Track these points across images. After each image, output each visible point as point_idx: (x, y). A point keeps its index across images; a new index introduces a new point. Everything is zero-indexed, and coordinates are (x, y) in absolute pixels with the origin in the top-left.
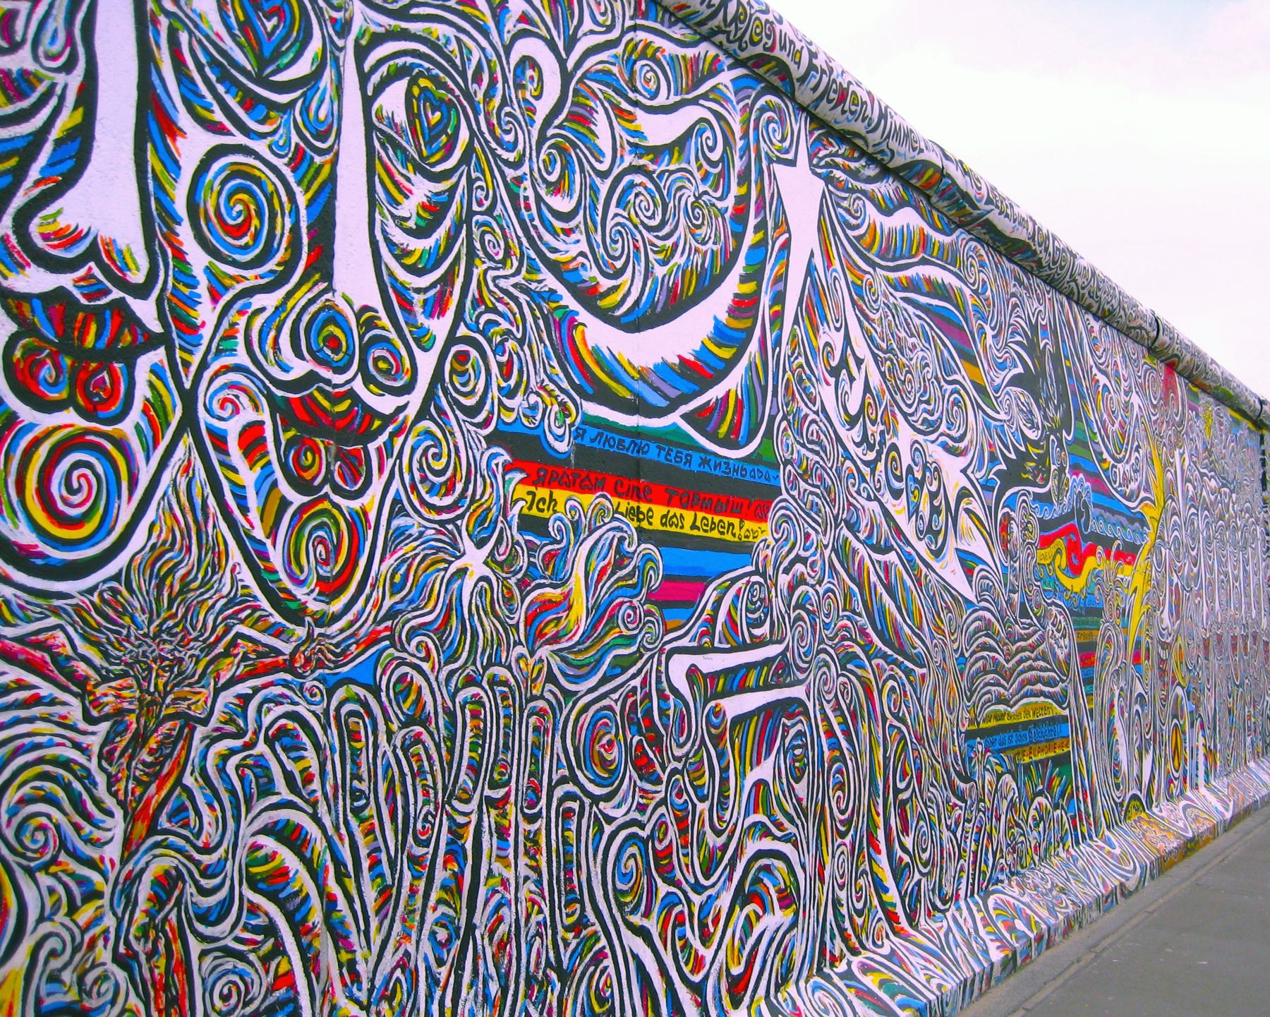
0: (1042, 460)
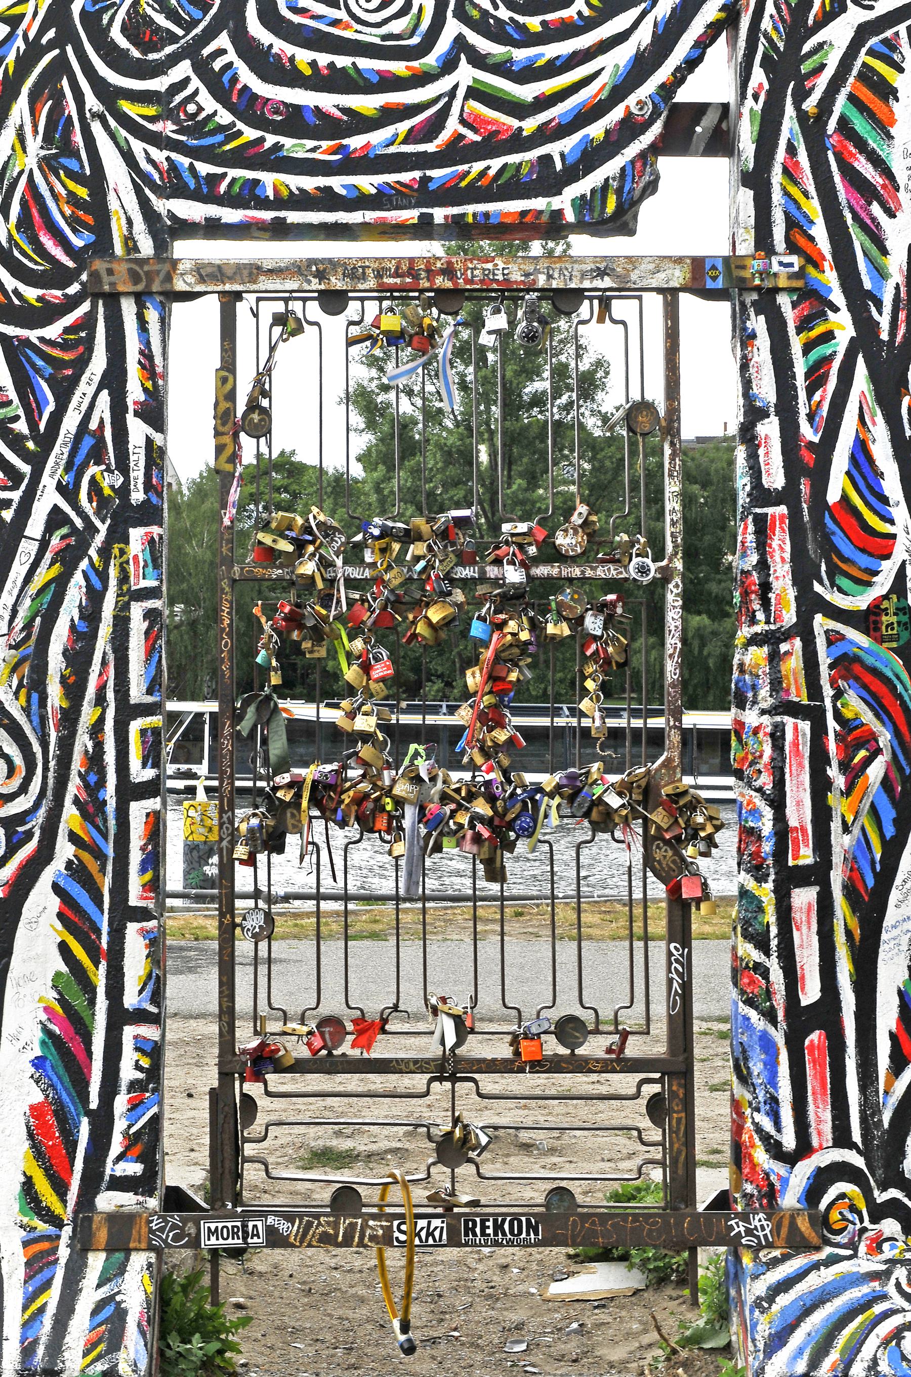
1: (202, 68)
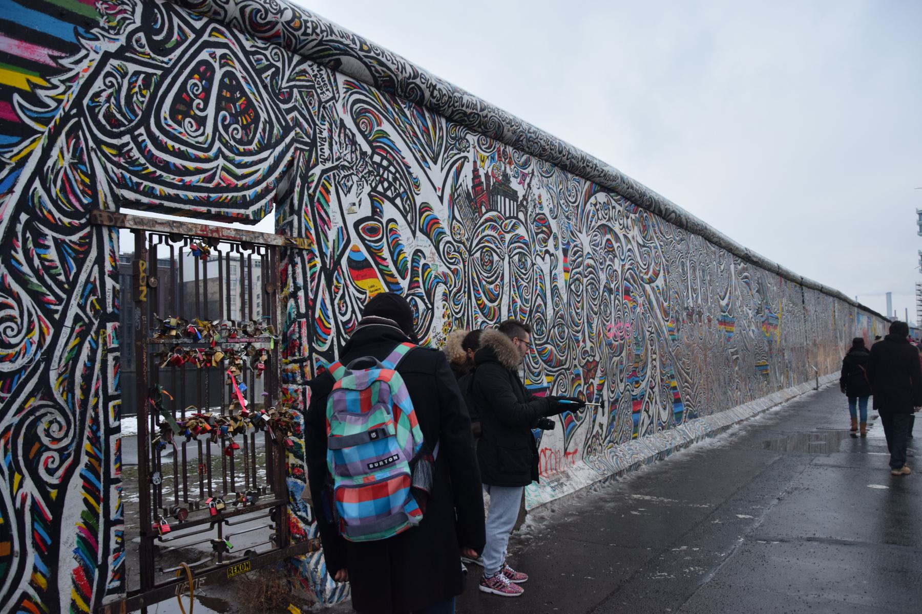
1: (135, 139)
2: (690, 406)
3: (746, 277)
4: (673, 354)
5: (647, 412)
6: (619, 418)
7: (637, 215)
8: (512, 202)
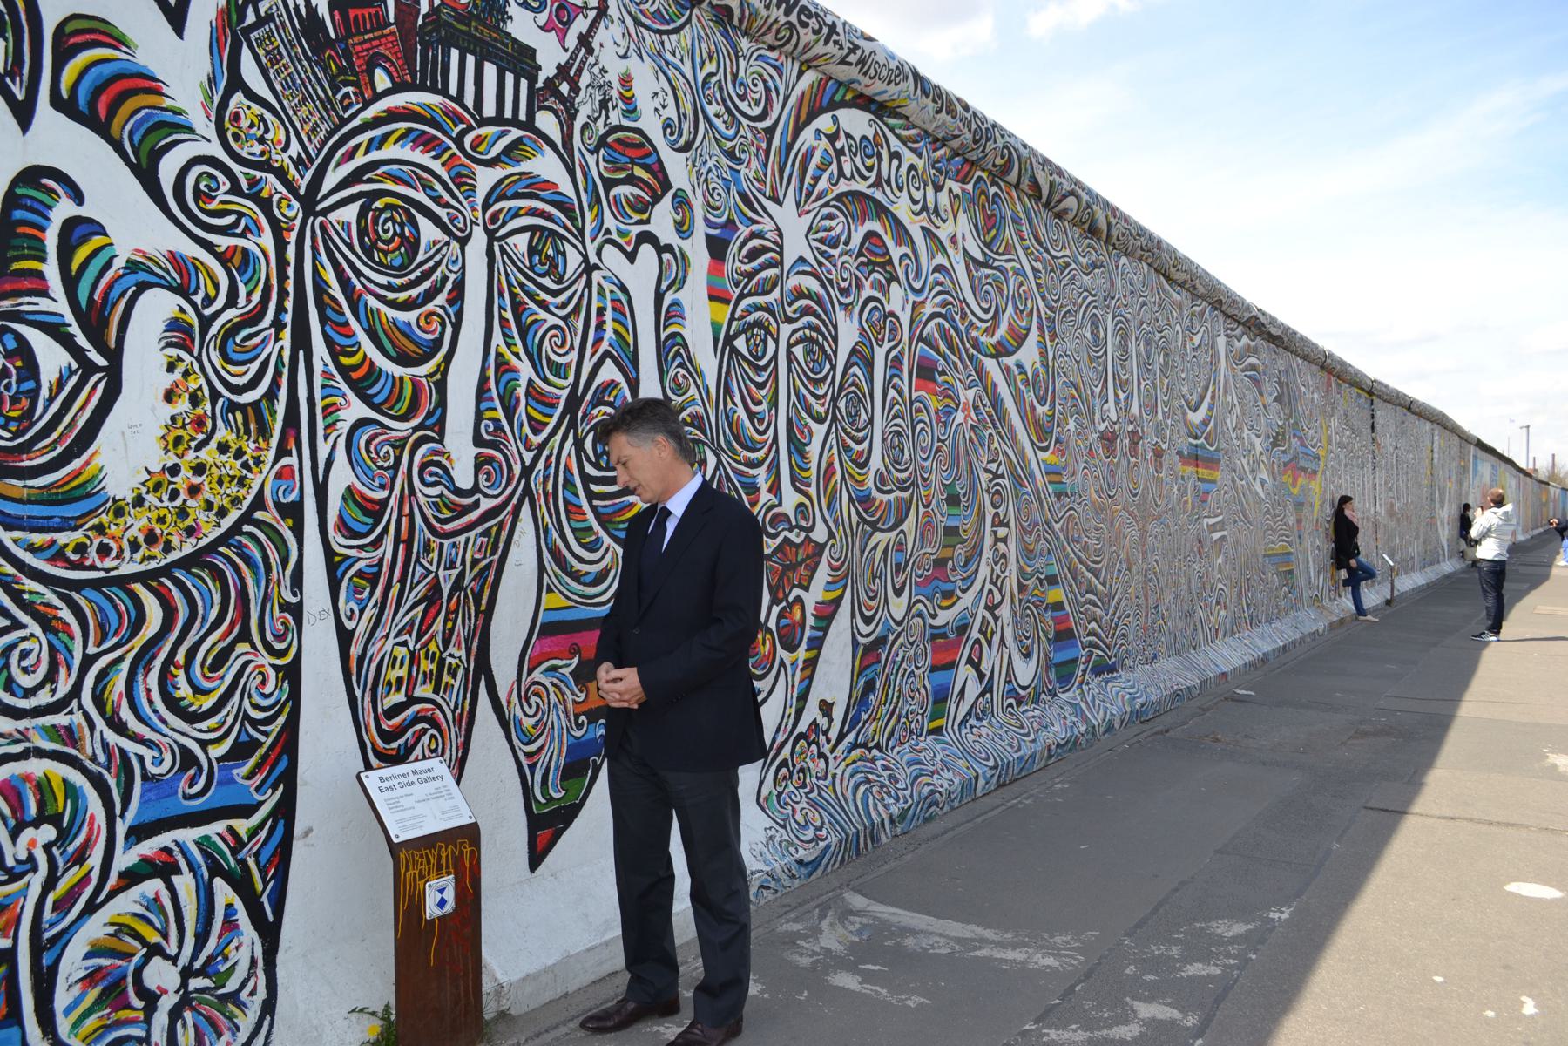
0: (1284, 433)
2: (1097, 647)
3: (1253, 368)
4: (1057, 527)
5: (977, 667)
6: (887, 684)
7: (969, 187)
8: (509, 78)
